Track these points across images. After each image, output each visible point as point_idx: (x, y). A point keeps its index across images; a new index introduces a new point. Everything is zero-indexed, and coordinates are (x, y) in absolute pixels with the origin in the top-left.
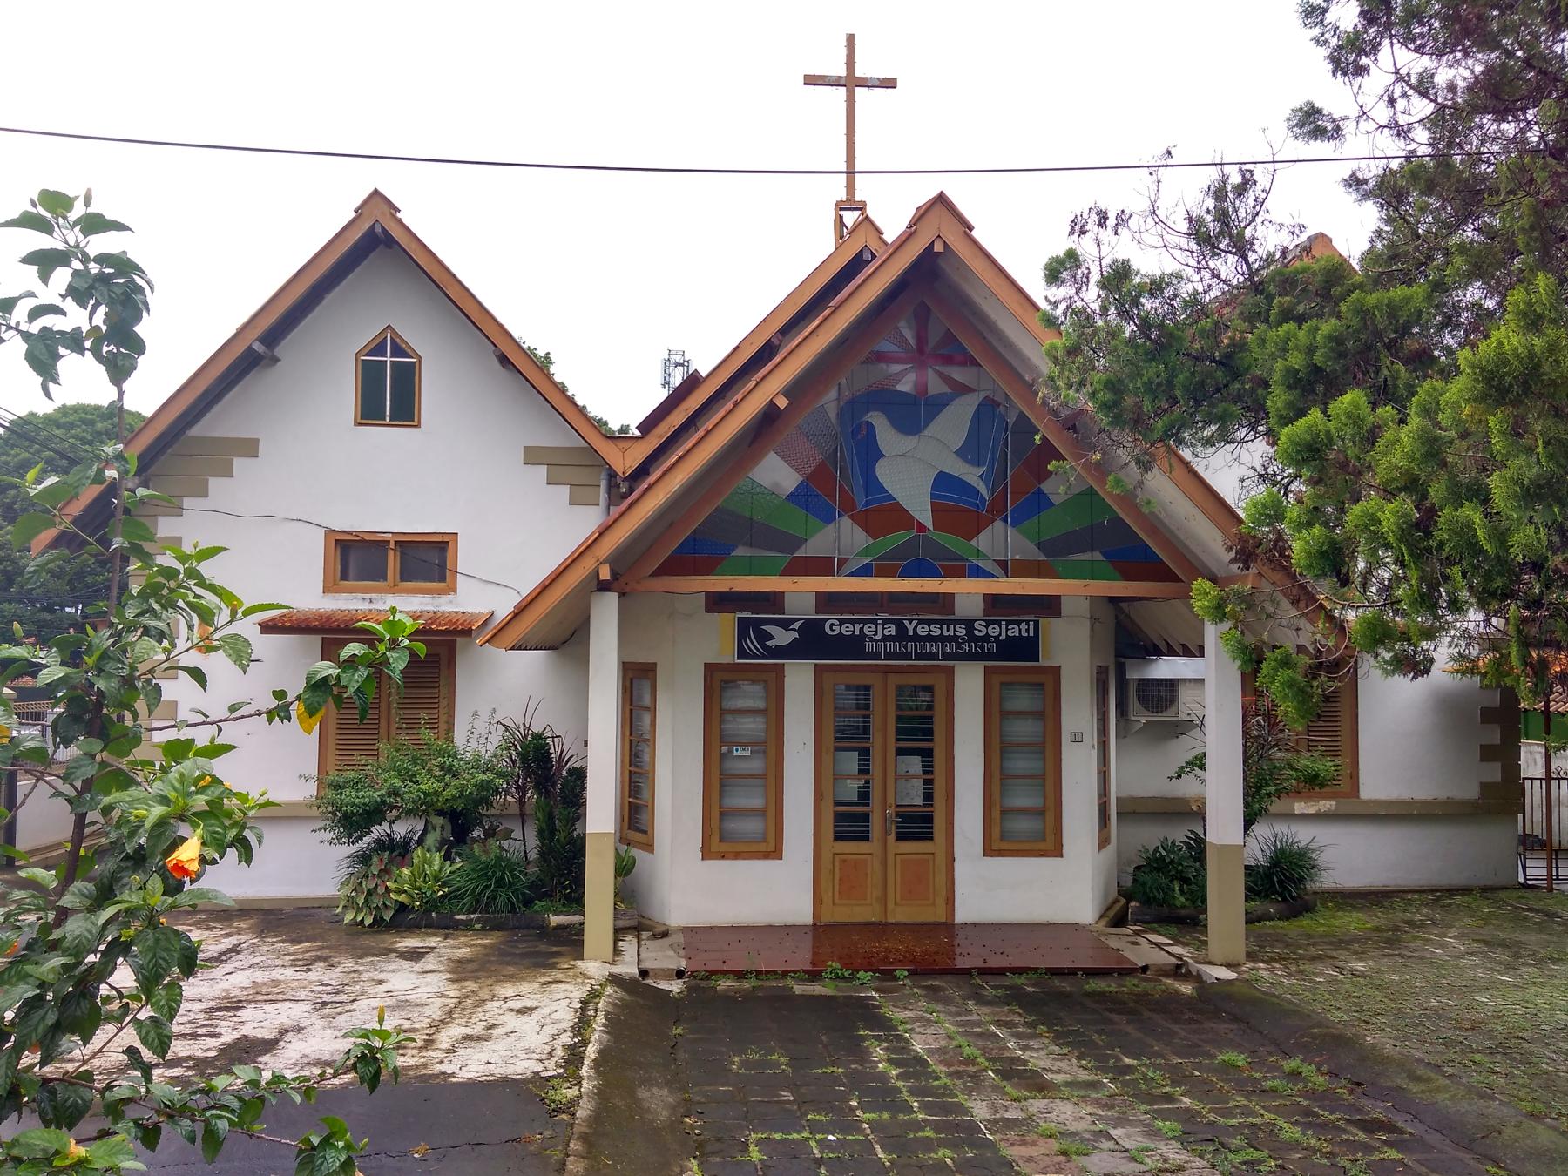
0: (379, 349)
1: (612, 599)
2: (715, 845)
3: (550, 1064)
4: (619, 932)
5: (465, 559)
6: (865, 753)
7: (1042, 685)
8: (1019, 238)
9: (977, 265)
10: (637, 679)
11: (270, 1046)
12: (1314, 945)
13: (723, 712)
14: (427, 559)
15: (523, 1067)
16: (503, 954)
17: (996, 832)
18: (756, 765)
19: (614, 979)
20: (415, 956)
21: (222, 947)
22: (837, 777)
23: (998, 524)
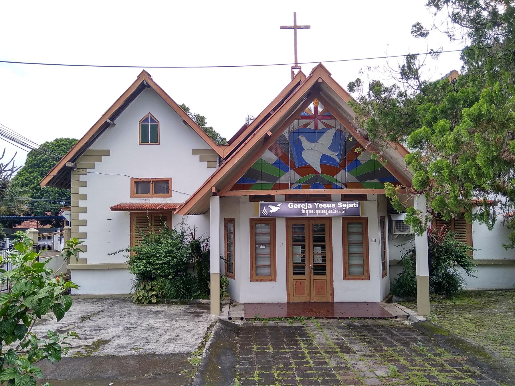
0: (146, 120)
1: (217, 198)
2: (254, 277)
3: (194, 348)
4: (222, 305)
5: (175, 186)
6: (303, 246)
7: (362, 223)
8: (342, 77)
9: (332, 86)
10: (229, 225)
11: (107, 342)
12: (455, 309)
13: (256, 234)
14: (163, 186)
15: (185, 349)
16: (185, 312)
17: (347, 272)
18: (267, 251)
19: (220, 321)
20: (158, 313)
21: (99, 310)
22: (294, 254)
23: (343, 171)
